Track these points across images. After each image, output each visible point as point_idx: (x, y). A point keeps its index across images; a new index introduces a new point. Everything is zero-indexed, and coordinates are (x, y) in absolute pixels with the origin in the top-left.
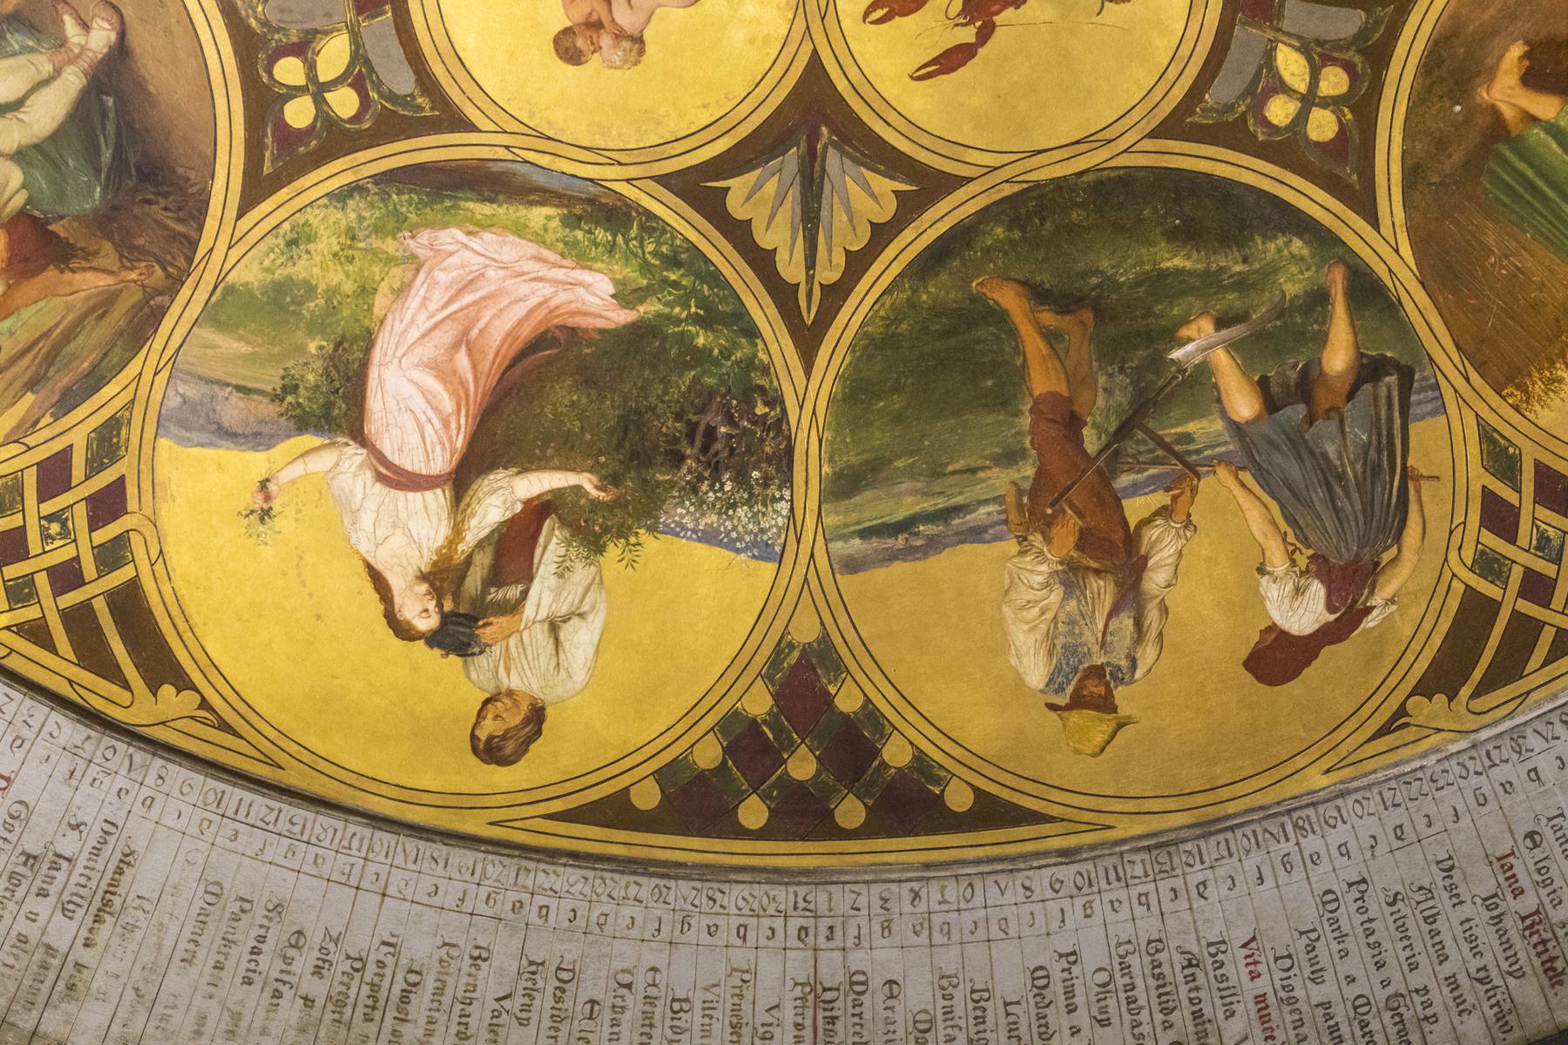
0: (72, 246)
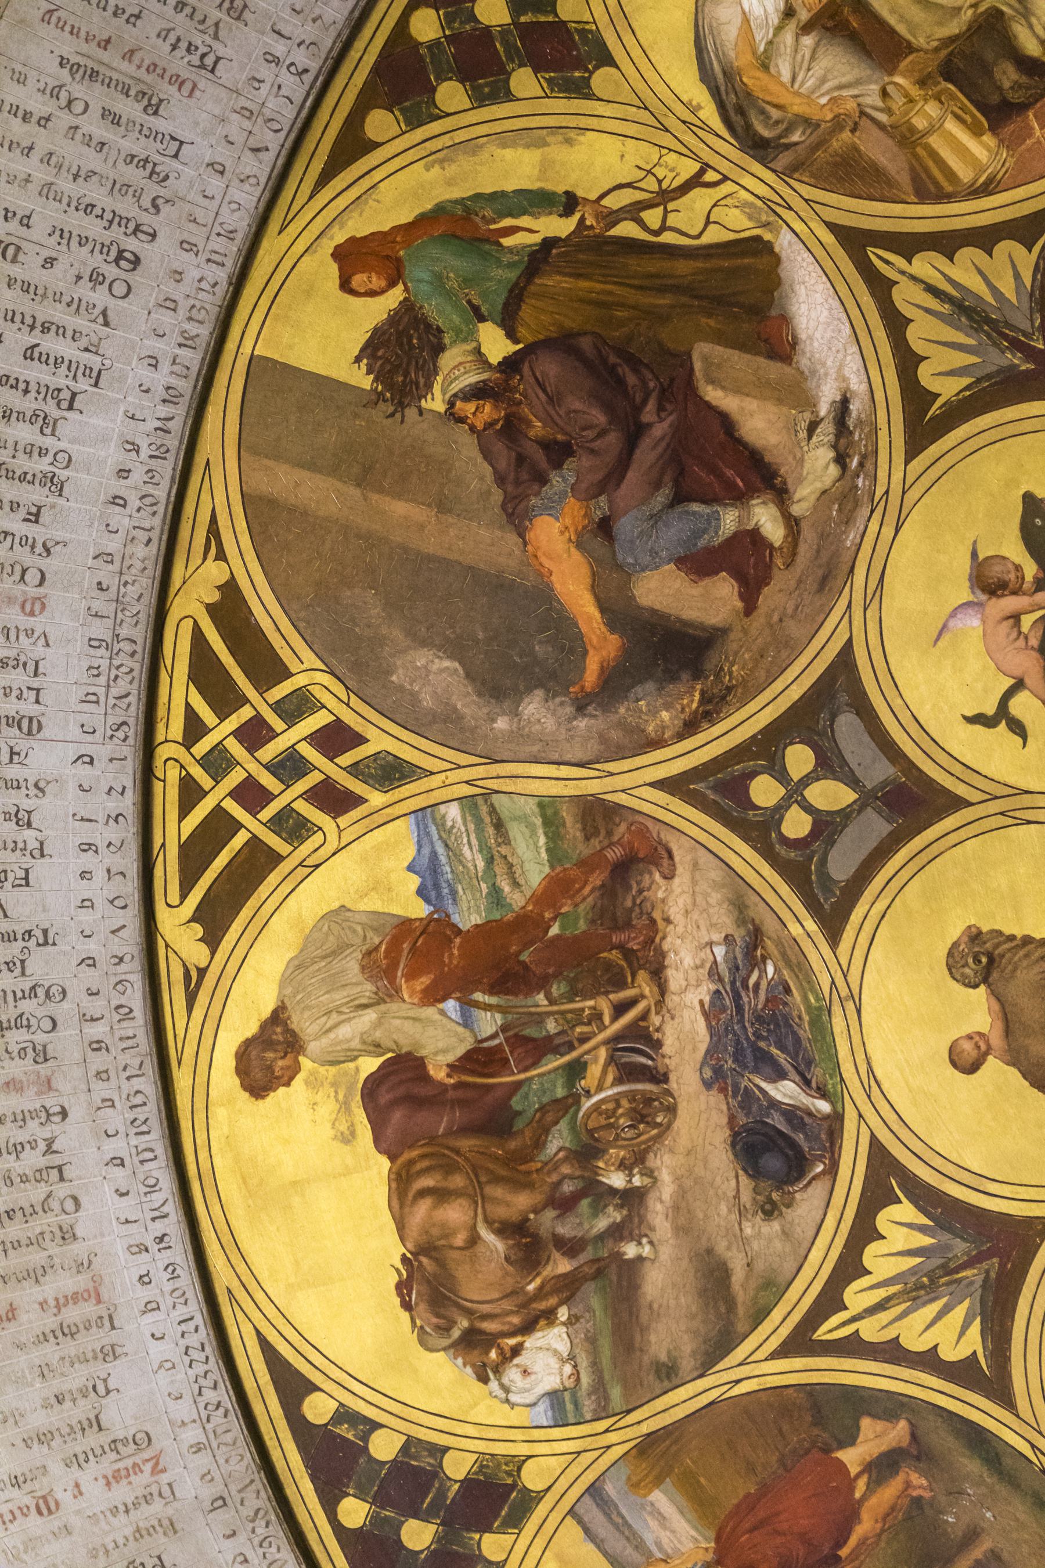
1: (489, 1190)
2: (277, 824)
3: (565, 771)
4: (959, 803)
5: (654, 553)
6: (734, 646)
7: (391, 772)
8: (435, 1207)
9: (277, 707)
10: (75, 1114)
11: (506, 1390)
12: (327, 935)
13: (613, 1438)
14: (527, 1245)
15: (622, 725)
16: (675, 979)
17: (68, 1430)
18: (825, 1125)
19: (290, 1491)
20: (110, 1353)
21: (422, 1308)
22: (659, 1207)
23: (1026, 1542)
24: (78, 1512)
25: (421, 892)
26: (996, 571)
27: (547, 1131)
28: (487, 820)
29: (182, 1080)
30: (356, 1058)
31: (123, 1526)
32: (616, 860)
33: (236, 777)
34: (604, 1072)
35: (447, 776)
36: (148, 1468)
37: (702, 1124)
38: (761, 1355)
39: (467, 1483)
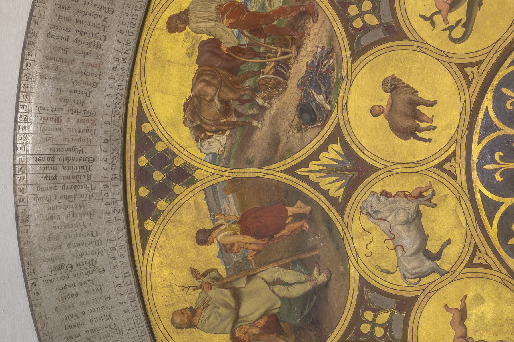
0: (284, 331)
1: (223, 88)
4: (407, 38)
8: (205, 86)
10: (116, 13)
11: (202, 147)
13: (226, 174)
14: (226, 109)
16: (303, 52)
18: (327, 113)
20: (95, 85)
21: (189, 112)
22: (269, 115)
24: (66, 126)
27: (247, 79)
29: (150, 18)
30: (202, 34)
34: (271, 69)
36: (91, 122)
37: (292, 97)
38: (278, 170)
39: (179, 168)
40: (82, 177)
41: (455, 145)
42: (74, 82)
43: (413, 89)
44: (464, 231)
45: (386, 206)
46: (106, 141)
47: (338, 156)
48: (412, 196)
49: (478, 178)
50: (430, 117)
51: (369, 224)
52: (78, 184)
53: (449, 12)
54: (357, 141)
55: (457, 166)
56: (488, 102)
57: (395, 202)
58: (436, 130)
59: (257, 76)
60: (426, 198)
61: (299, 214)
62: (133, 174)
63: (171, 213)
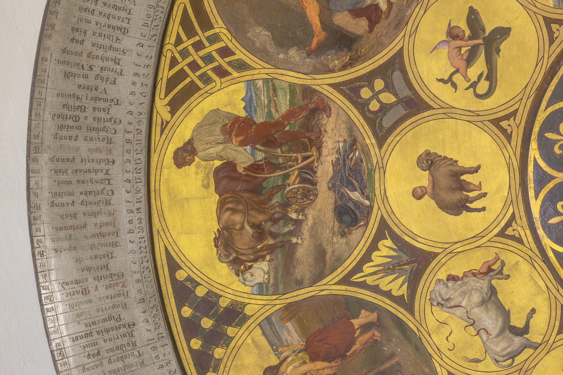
1: (250, 212)
2: (201, 77)
3: (300, 75)
4: (430, 108)
5: (342, 6)
6: (363, 43)
7: (241, 66)
8: (231, 215)
9: (208, 38)
11: (245, 280)
12: (211, 117)
13: (277, 302)
14: (260, 233)
15: (321, 63)
16: (325, 151)
17: (97, 268)
18: (367, 209)
19: (166, 301)
20: (115, 245)
21: (221, 247)
22: (306, 227)
23: (410, 361)
24: (95, 296)
25: (245, 108)
26: (456, 31)
27: (273, 195)
28: (271, 88)
29: (154, 158)
30: (214, 160)
31: (109, 303)
32: (312, 107)
33: (190, 59)
34: (296, 179)
35: (261, 71)
36: (121, 285)
37: (326, 202)
38: (331, 283)
39: (227, 309)
40: (126, 346)
41: (511, 206)
42: (92, 247)
43: (451, 159)
44: (546, 295)
45: (456, 291)
46: (142, 300)
47: (392, 251)
48: (481, 273)
49: (545, 235)
50: (477, 184)
51: (443, 315)
52: (124, 354)
53: (467, 68)
54: (407, 230)
55: (519, 228)
56: (534, 152)
57: (465, 284)
58: (487, 196)
59: (283, 190)
60: (497, 271)
61: (366, 323)
62: (180, 328)
63: (231, 358)
